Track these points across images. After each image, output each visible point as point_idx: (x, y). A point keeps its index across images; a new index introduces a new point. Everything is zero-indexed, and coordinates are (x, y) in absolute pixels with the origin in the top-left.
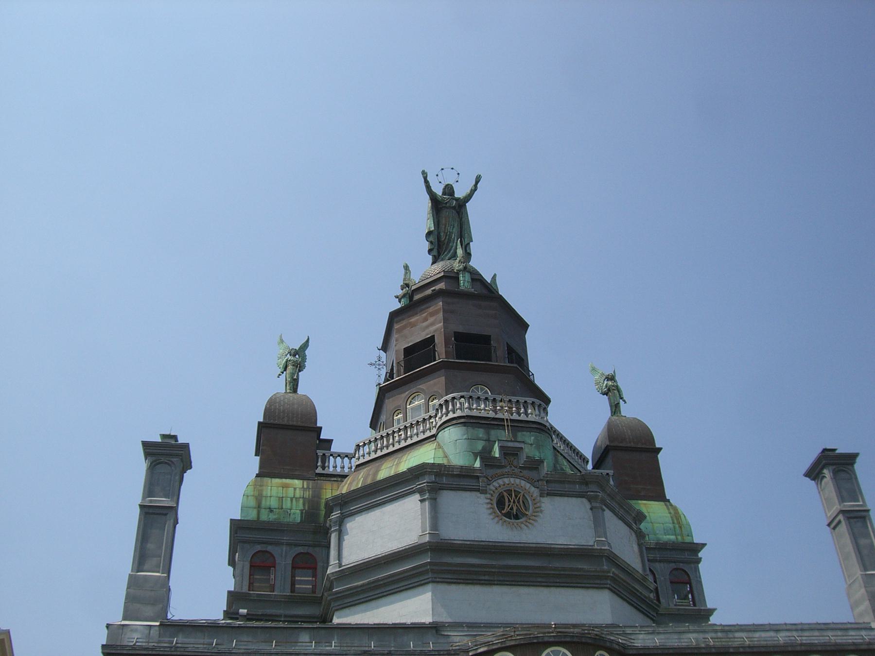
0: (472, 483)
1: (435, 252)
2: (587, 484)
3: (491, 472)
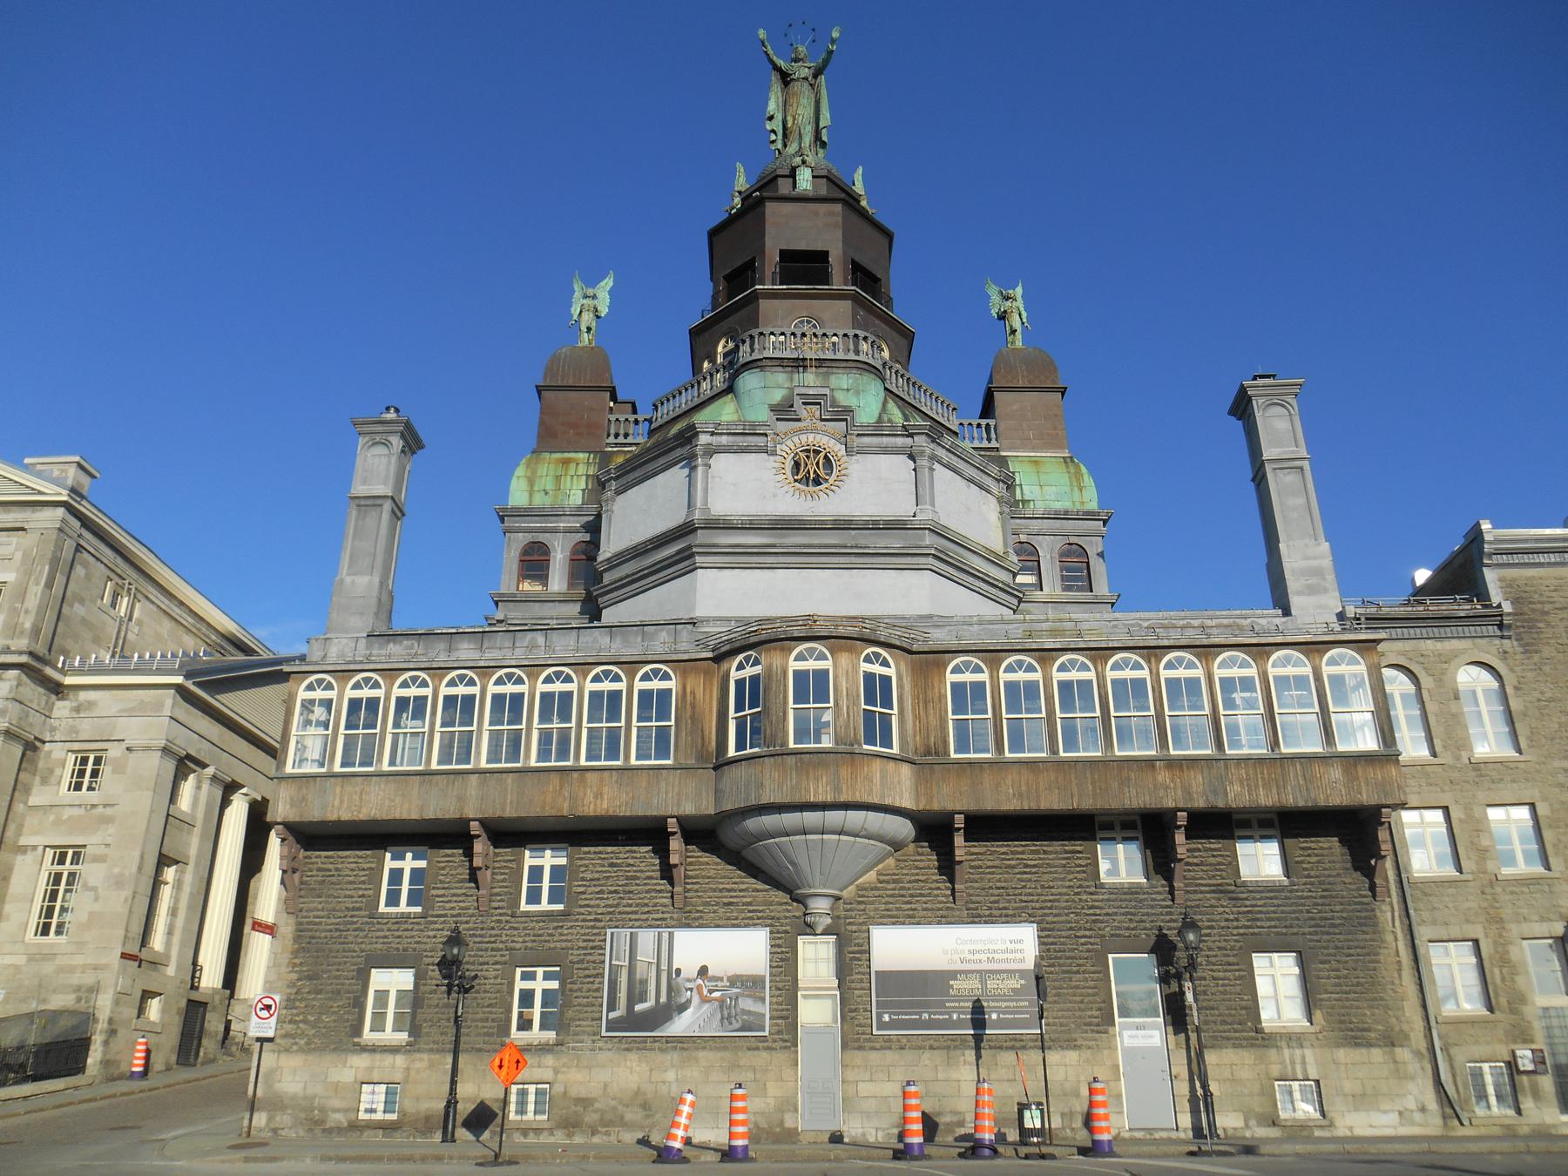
2: (911, 436)
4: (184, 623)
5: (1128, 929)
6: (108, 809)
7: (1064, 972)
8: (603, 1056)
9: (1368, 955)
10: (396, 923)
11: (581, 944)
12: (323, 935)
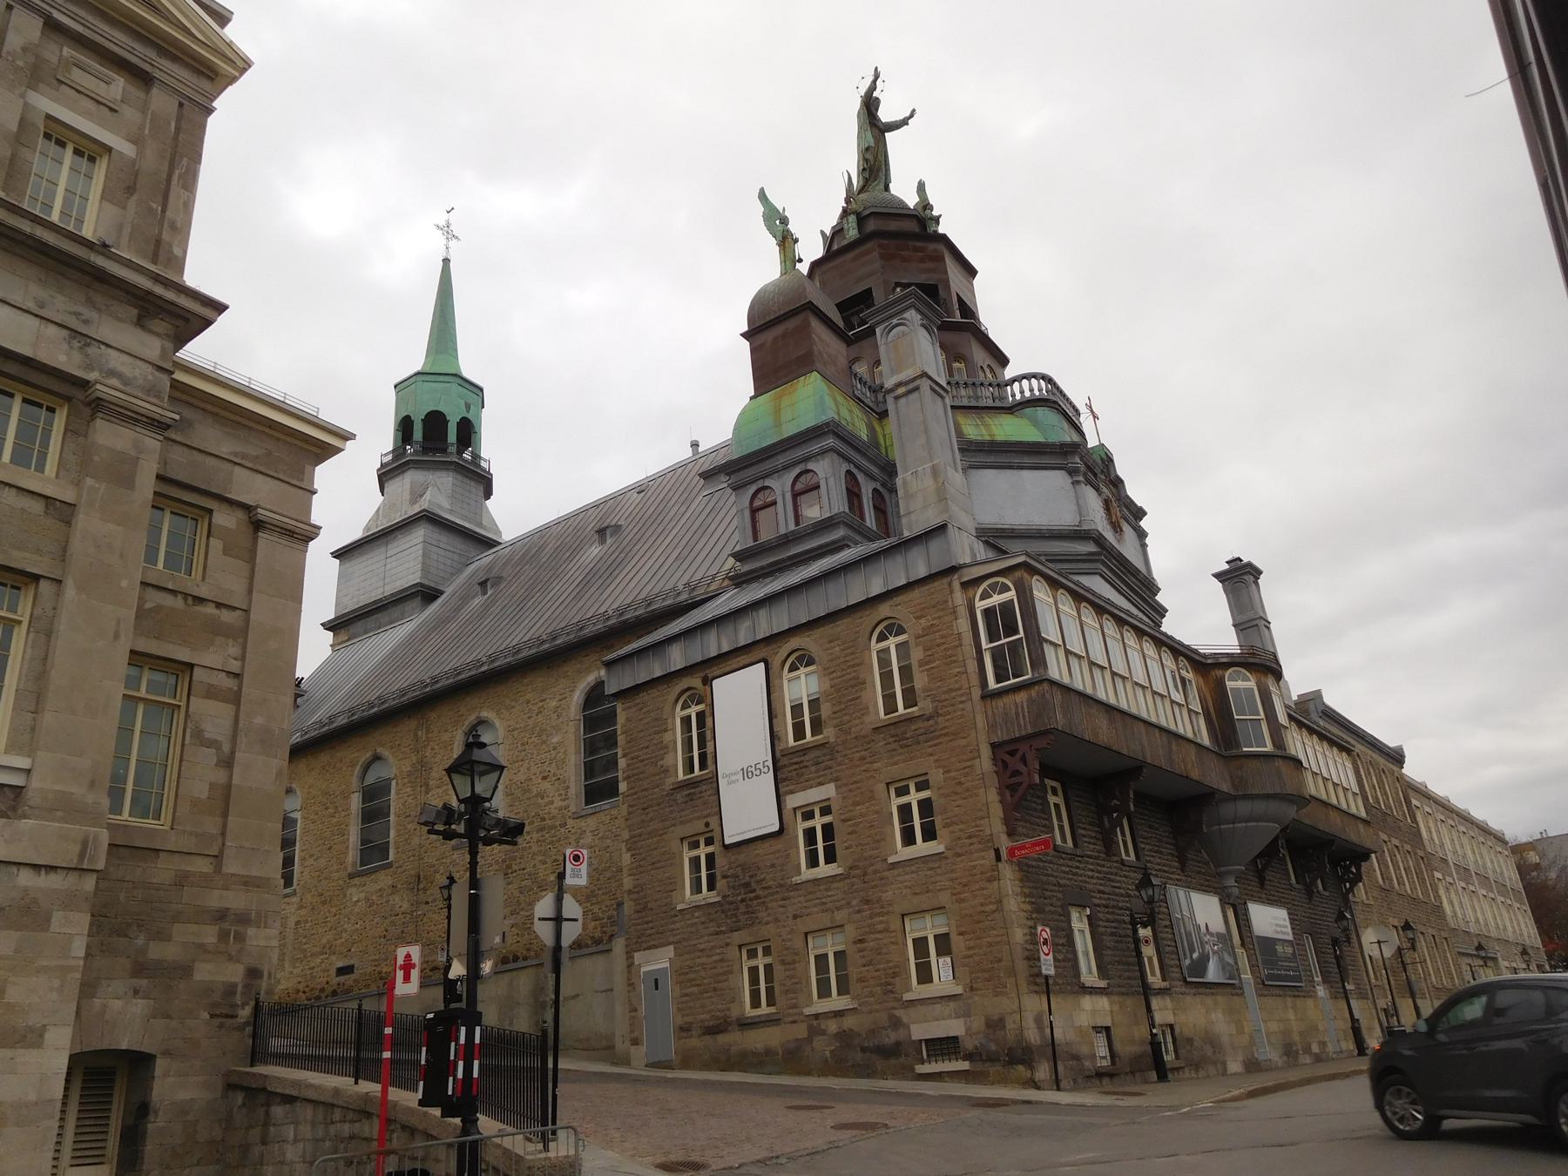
8: (1189, 999)
10: (1070, 859)
12: (1034, 863)
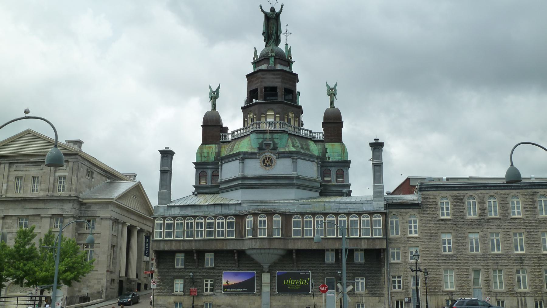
0: (254, 156)
1: (267, 41)
3: (261, 152)
4: (103, 174)
5: (330, 272)
6: (98, 234)
7: (316, 281)
9: (378, 278)
11: (217, 274)
